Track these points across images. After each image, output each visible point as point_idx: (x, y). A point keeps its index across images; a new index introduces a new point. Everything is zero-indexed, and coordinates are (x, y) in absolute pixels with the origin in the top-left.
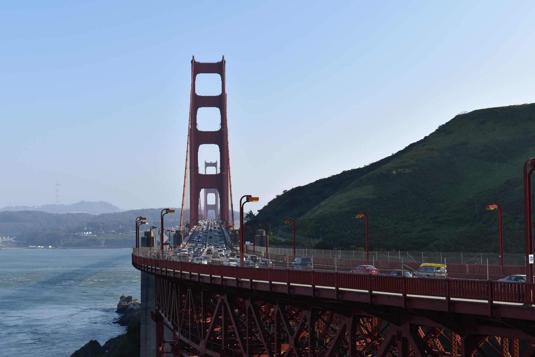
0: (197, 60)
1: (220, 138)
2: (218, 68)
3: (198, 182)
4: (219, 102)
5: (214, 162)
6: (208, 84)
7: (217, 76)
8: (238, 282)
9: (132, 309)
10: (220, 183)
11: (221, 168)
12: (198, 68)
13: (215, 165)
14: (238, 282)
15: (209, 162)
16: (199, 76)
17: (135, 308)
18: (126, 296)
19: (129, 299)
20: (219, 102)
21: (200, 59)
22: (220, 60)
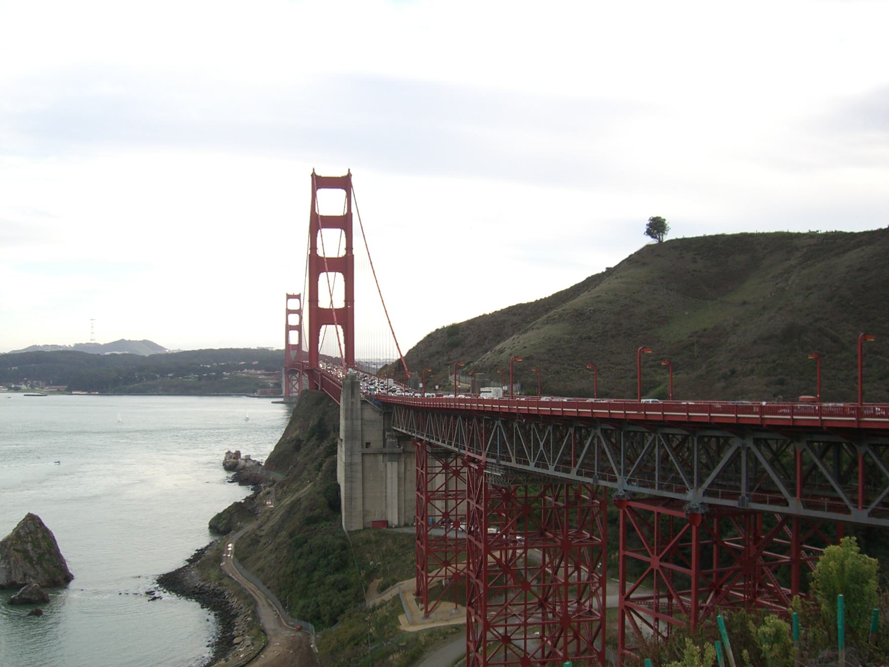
0: (318, 173)
1: (344, 265)
2: (344, 183)
3: (320, 317)
4: (344, 223)
5: (296, 293)
6: (332, 202)
7: (341, 193)
8: (859, 422)
9: (244, 468)
10: (344, 318)
11: (346, 301)
12: (319, 182)
13: (298, 297)
14: (859, 422)
15: (291, 293)
16: (321, 192)
17: (248, 465)
18: (233, 451)
19: (238, 454)
20: (344, 223)
21: (322, 173)
22: (345, 173)
